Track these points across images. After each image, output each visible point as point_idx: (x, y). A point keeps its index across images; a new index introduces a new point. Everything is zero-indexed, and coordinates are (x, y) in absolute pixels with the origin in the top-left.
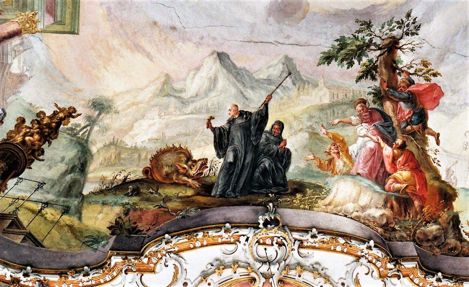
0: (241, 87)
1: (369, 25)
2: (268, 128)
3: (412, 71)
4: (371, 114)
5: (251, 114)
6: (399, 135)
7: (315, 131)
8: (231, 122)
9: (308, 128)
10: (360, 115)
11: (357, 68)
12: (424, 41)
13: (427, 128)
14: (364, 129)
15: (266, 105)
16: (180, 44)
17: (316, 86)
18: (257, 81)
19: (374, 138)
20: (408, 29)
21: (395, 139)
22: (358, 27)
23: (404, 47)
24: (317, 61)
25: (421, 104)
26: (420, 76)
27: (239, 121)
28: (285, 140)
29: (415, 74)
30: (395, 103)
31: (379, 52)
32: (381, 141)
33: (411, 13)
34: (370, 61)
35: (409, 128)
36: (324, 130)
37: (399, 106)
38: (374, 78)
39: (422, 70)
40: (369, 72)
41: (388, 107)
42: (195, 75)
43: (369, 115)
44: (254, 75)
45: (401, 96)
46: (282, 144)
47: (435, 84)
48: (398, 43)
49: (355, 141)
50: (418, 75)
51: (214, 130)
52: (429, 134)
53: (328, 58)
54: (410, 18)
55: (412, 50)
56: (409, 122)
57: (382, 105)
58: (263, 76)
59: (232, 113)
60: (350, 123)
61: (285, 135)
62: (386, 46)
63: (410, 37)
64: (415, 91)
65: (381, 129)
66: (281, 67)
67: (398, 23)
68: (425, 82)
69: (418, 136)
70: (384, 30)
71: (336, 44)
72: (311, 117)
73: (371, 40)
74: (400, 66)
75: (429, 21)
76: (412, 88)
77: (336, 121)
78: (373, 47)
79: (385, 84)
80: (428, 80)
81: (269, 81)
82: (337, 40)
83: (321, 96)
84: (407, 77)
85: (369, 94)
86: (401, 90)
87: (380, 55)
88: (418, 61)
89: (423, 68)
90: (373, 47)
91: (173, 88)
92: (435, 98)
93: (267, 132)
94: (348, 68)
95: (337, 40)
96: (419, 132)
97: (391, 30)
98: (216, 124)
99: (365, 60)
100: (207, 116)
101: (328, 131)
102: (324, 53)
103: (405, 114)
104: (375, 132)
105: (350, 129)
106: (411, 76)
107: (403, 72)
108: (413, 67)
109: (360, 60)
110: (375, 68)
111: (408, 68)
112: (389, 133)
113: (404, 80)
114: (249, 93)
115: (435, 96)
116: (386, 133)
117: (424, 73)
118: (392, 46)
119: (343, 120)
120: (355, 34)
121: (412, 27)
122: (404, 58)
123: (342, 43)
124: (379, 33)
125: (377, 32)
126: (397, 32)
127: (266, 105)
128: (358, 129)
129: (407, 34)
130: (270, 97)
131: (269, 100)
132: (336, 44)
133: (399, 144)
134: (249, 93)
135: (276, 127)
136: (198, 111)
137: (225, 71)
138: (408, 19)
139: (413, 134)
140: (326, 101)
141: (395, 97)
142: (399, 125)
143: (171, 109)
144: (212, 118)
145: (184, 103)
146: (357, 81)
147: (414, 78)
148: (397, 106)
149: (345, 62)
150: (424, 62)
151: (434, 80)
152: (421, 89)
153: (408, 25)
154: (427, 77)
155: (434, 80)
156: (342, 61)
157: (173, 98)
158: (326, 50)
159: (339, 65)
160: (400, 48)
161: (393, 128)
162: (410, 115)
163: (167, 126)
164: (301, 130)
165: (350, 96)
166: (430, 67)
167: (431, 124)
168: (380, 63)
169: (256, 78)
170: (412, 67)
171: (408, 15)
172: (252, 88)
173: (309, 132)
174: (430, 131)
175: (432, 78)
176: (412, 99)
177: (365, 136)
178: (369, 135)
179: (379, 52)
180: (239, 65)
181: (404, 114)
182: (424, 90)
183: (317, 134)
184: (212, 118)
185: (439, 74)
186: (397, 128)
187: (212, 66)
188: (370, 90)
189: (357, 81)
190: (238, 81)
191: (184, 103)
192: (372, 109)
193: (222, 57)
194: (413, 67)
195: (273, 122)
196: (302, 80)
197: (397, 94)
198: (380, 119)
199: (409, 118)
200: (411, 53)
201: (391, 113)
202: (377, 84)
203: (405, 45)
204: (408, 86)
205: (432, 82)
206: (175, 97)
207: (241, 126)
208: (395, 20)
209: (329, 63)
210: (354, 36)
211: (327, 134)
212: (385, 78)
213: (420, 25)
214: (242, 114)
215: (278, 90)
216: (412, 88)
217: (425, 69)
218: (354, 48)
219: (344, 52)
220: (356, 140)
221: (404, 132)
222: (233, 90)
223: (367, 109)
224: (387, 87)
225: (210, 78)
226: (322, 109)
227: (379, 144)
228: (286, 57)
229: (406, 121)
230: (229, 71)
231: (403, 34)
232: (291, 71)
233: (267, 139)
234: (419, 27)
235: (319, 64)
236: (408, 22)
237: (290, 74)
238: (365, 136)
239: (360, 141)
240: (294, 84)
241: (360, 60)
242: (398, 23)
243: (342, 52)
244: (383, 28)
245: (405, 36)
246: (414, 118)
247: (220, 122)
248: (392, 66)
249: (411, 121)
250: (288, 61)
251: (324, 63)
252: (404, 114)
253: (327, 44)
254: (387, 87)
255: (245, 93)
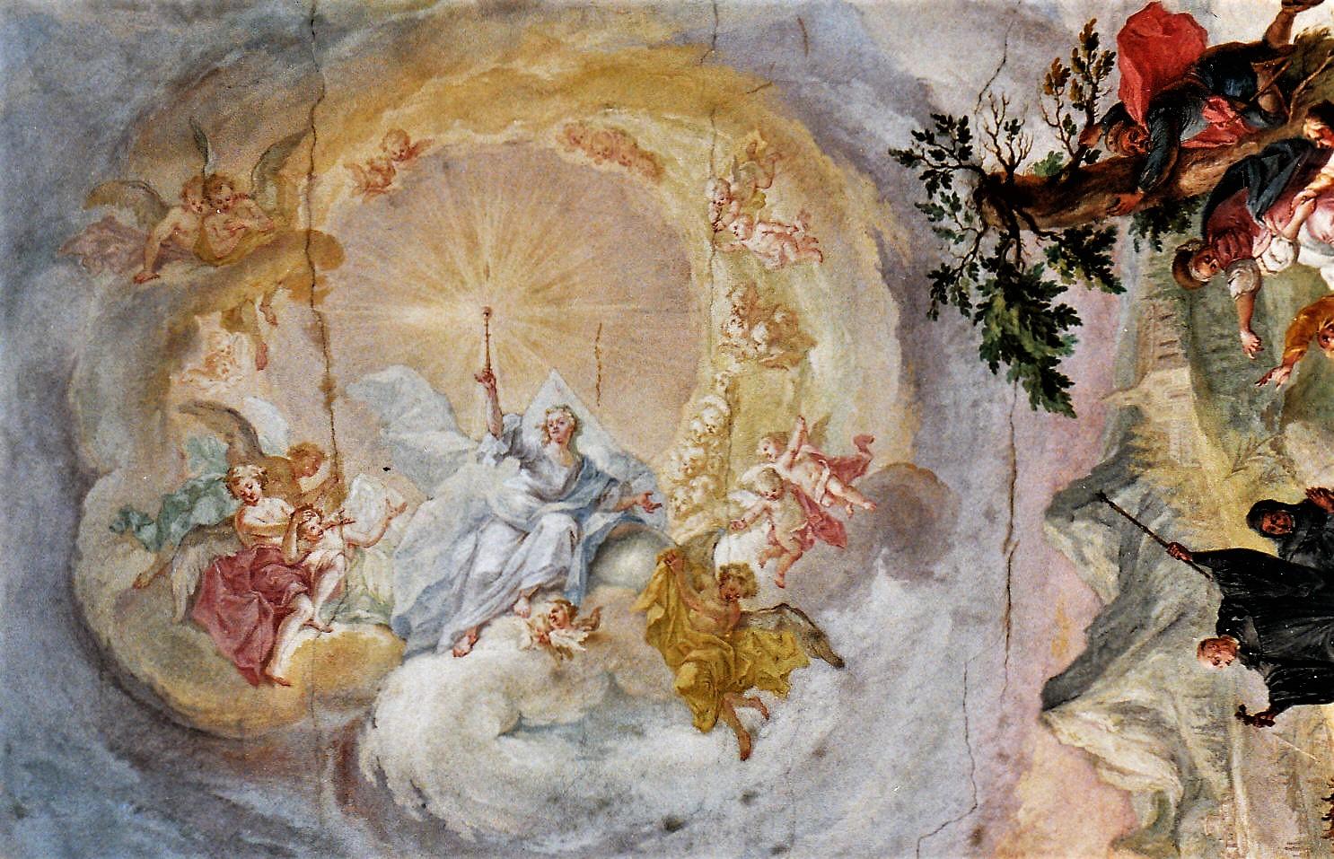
0: (1145, 636)
1: (944, 277)
2: (1269, 548)
3: (1080, 120)
4: (1222, 233)
5: (1226, 603)
6: (1289, 132)
7: (1281, 401)
8: (1251, 657)
9: (1270, 426)
10: (1228, 267)
11: (1077, 294)
12: (985, 97)
13: (1265, 41)
14: (1271, 252)
15: (1198, 559)
16: (1021, 814)
17: (1135, 412)
18: (1125, 588)
19: (1299, 213)
20: (951, 153)
21: (1302, 144)
22: (951, 312)
23: (1006, 155)
24: (1061, 418)
25: (1185, 75)
26: (1095, 89)
27: (1252, 632)
28: (1310, 492)
29: (1088, 108)
30: (1183, 158)
31: (1026, 235)
32: (1309, 190)
33: (900, 152)
34: (1053, 256)
35: (1265, 102)
36: (1277, 375)
37: (1195, 144)
38: (1108, 238)
39: (1075, 85)
40: (1088, 255)
41: (1194, 180)
42: (1111, 768)
43: (1228, 236)
44: (1107, 602)
45: (1163, 142)
46: (1323, 502)
47: (1120, 37)
48: (996, 177)
49: (1313, 273)
50: (1094, 97)
51: (1277, 707)
52: (1285, 33)
53: (1050, 388)
54: (918, 152)
55: (1014, 129)
56: (1247, 104)
57: (1191, 202)
58: (1110, 575)
59: (1225, 656)
60: (1254, 295)
61: (1291, 494)
62: (1005, 216)
63: (975, 145)
64: (1144, 97)
65: (1268, 193)
66: (1079, 526)
67: (932, 188)
68: (1115, 72)
69: (1291, 67)
70: (955, 228)
71: (1004, 368)
72: (1236, 421)
73: (990, 264)
74: (1066, 159)
75: (923, 88)
76: (1136, 112)
77: (1246, 339)
78: (1010, 256)
79: (1126, 198)
80: (1108, 59)
81: (1124, 556)
82: (994, 367)
83: (1170, 390)
84: (1100, 131)
85: (1156, 245)
86: (1141, 143)
87: (1035, 229)
88: (1049, 103)
89: (1068, 86)
90: (1010, 256)
91: (1155, 826)
92: (1165, 32)
93: (1284, 550)
94: (1077, 322)
95: (994, 367)
96: (1278, 67)
97: (956, 206)
98: (1260, 700)
99: (1050, 275)
100: (1237, 728)
101: (1279, 361)
102: (1034, 401)
103: (1220, 119)
104: (1281, 212)
105: (1268, 294)
106: (1097, 121)
107: (1083, 148)
108: (1068, 116)
109: (1052, 290)
110: (1074, 238)
111: (1073, 132)
112: (1283, 164)
113: (1110, 139)
114: (1163, 610)
115: (1158, 33)
116: (1285, 175)
117: (1087, 78)
118: (1005, 196)
119: (1242, 319)
120: (973, 316)
121: (944, 142)
122: (1042, 147)
123: (1001, 350)
124: (966, 243)
125: (964, 248)
126: (961, 187)
127: (1198, 559)
128: (1272, 266)
129: (965, 153)
130: (1177, 550)
131: (1181, 548)
132: (1004, 368)
133: (1319, 127)
134: (1163, 610)
135: (1267, 523)
136: (1222, 755)
137: (1098, 685)
138: (919, 158)
139: (1286, 85)
140: (1182, 377)
141: (1165, 161)
142: (1257, 135)
143: (1217, 827)
144: (1241, 713)
145: (1196, 791)
146: (1119, 290)
147: (1101, 109)
148: (1195, 150)
149: (1061, 334)
150: (1050, 85)
151: (1107, 43)
152: (1137, 81)
153: (938, 155)
154: (1098, 68)
155: (1107, 43)
156: (1055, 343)
157: (1187, 824)
158: (1024, 396)
159: (1069, 352)
160: (1011, 167)
161: (1269, 152)
162: (1225, 104)
163: (1267, 838)
164: (1278, 448)
165: (1164, 305)
166: (1067, 63)
167: (1252, 33)
168: (1058, 224)
169: (1115, 594)
170: (1068, 122)
171: (908, 159)
172: (1148, 602)
173: (1284, 422)
174: (1276, 30)
175: (1100, 51)
176: (1171, 101)
177: (1295, 244)
178: (1289, 229)
179: (1026, 235)
180: (1077, 647)
181: (1221, 125)
182: (1139, 67)
183: (1289, 394)
184: (1241, 713)
185: (1088, 28)
186: (1267, 141)
187: (1087, 723)
188: (1145, 245)
189: (1119, 290)
190: (1128, 642)
191: (1196, 791)
192: (1204, 232)
193: (1055, 697)
194: (1068, 116)
195: (1253, 534)
196: (1119, 457)
197: (1157, 156)
198: (1240, 202)
199: (1232, 107)
200: (1025, 130)
201: (1220, 167)
202: (1124, 224)
203: (998, 154)
204: (1130, 123)
205: (1114, 47)
206: (1178, 819)
207: (1266, 628)
208: (923, 200)
209: (1065, 382)
210: (979, 317)
211: (1288, 363)
212: (1105, 201)
213: (936, 117)
214: (1226, 626)
215: (1153, 527)
216: (1136, 112)
217: (1075, 76)
218: (1014, 312)
219: (1029, 339)
220: (1308, 270)
221: (1278, 117)
222: (1155, 657)
223: (1205, 245)
224: (1133, 191)
225: (1120, 723)
226: (1207, 388)
227: (1320, 194)
228: (1052, 512)
229: (1242, 114)
230: (1099, 672)
231: (966, 167)
232: (1084, 497)
233: (1307, 548)
234: (942, 118)
235: (1069, 412)
236: (927, 156)
237: (1101, 497)
238: (1295, 244)
239: (1309, 257)
240: (1133, 480)
241: (1052, 290)
242: (932, 188)
243: (1029, 347)
244: (949, 233)
245: (973, 159)
246: (1233, 90)
247: (1256, 691)
248: (1063, 188)
249: (1244, 98)
250: (1064, 506)
251: (1066, 397)
252: (1221, 125)
253: (1008, 395)
254: (1133, 191)
255: (1164, 622)
